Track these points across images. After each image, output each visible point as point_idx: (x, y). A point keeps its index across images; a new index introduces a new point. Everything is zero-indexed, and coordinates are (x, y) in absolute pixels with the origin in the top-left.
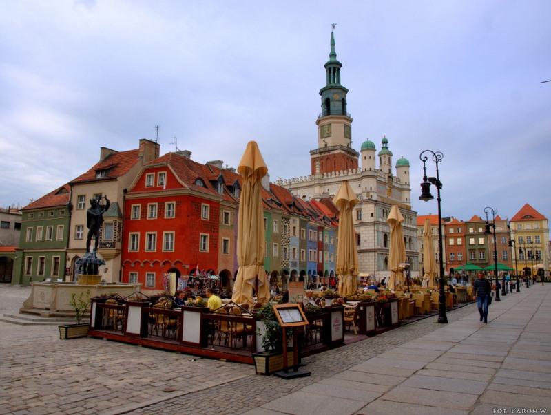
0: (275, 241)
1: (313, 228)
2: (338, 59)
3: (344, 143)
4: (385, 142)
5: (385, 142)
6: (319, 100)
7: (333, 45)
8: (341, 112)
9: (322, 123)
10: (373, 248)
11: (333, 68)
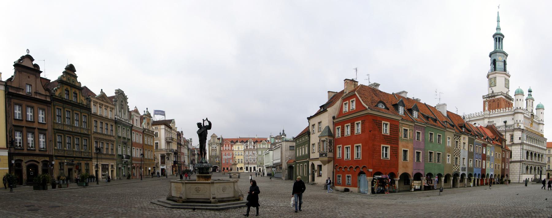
2: (502, 32)
3: (505, 91)
6: (489, 61)
7: (498, 21)
8: (503, 70)
11: (498, 38)
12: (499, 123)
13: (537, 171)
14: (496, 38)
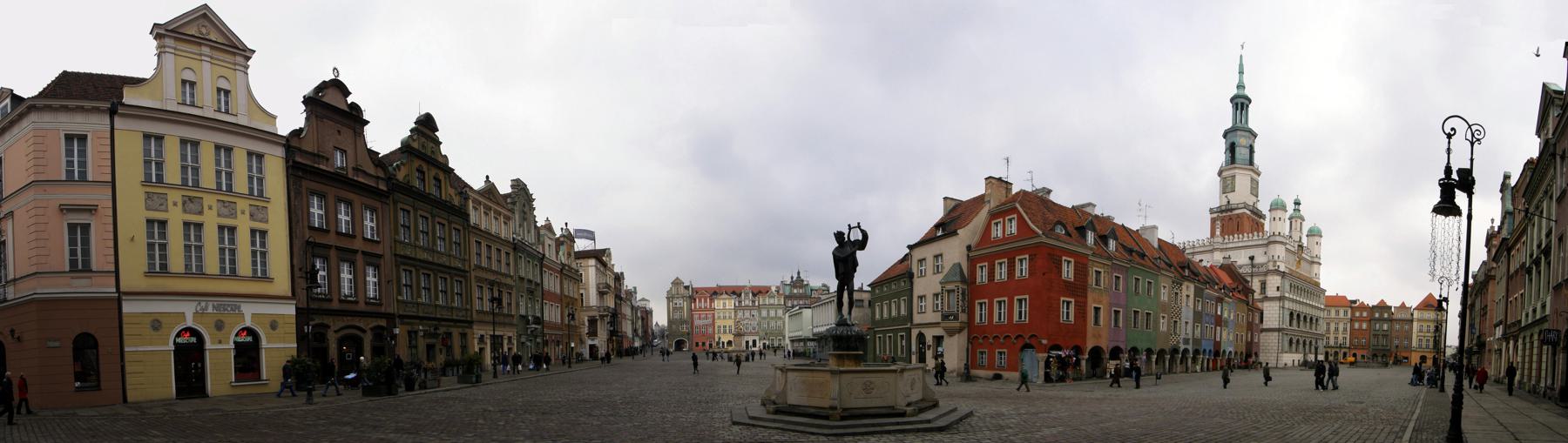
2: (1247, 92)
3: (1251, 200)
4: (1297, 203)
5: (1297, 203)
6: (1222, 145)
7: (1241, 72)
11: (1241, 103)
12: (1240, 259)
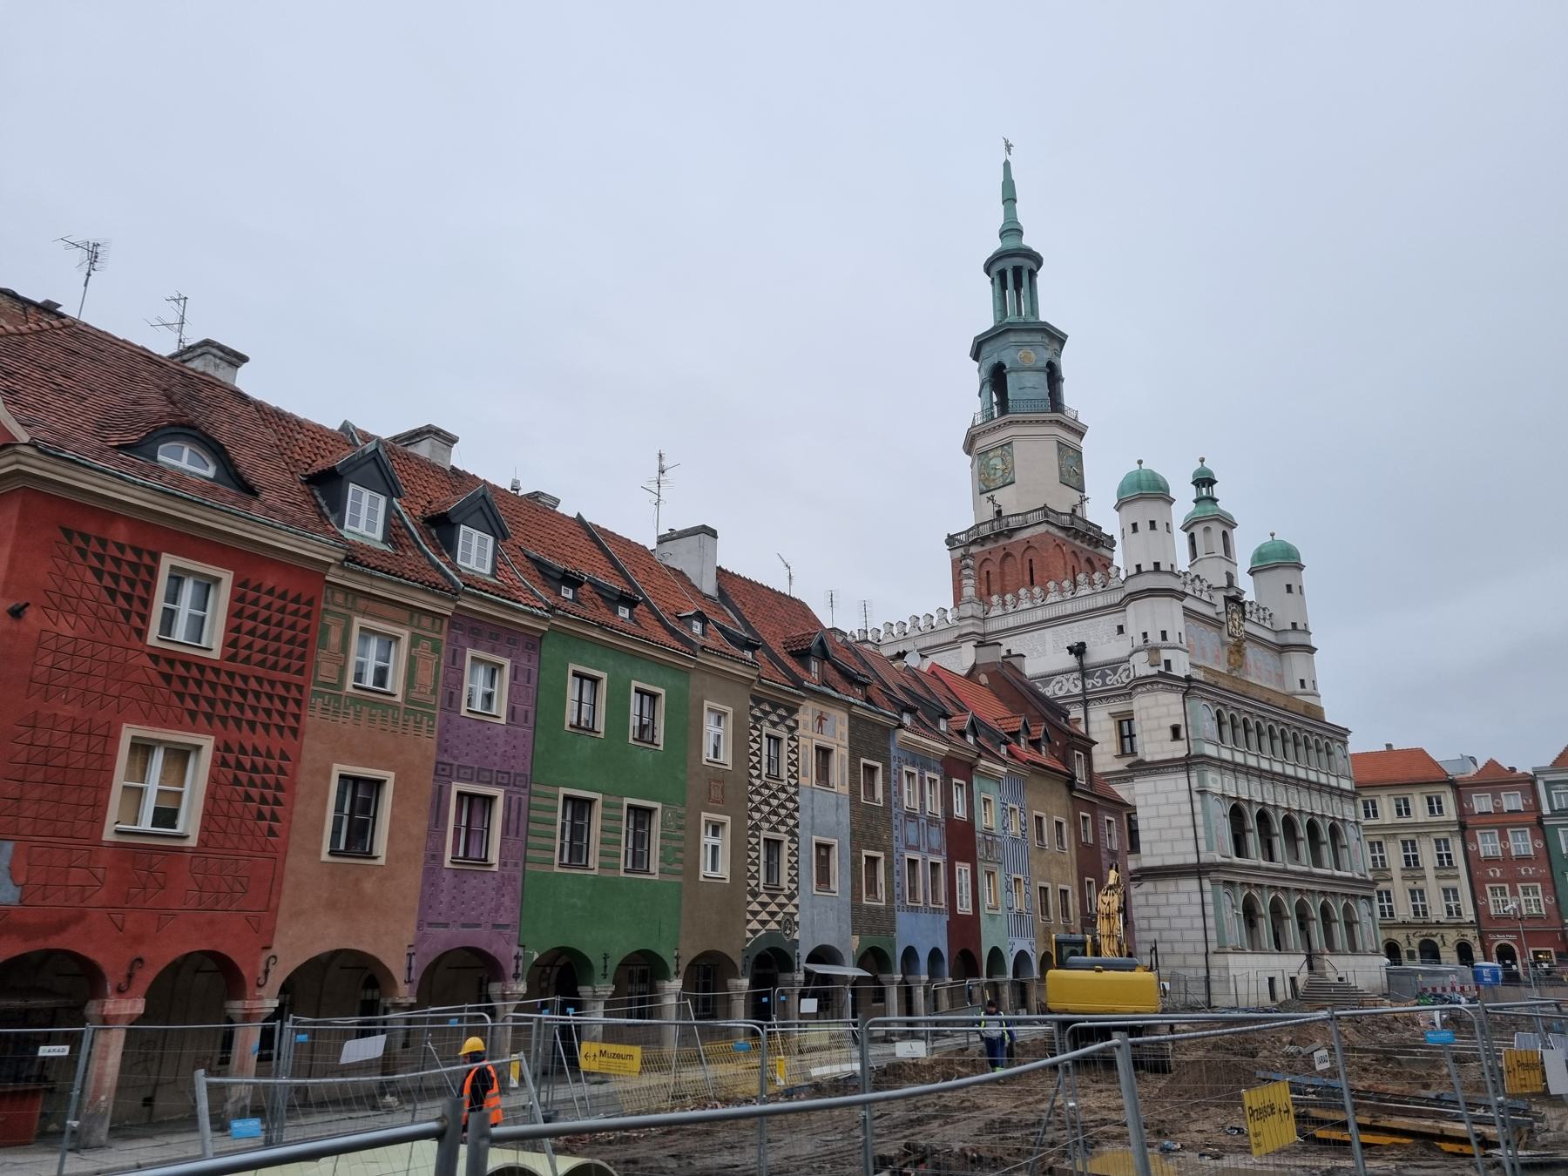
0: (720, 805)
1: (921, 759)
2: (1028, 241)
3: (1062, 501)
4: (1204, 481)
5: (1204, 481)
7: (1009, 199)
9: (980, 443)
10: (1192, 859)
11: (1014, 269)
12: (1042, 657)
13: (1316, 929)
14: (1002, 274)
